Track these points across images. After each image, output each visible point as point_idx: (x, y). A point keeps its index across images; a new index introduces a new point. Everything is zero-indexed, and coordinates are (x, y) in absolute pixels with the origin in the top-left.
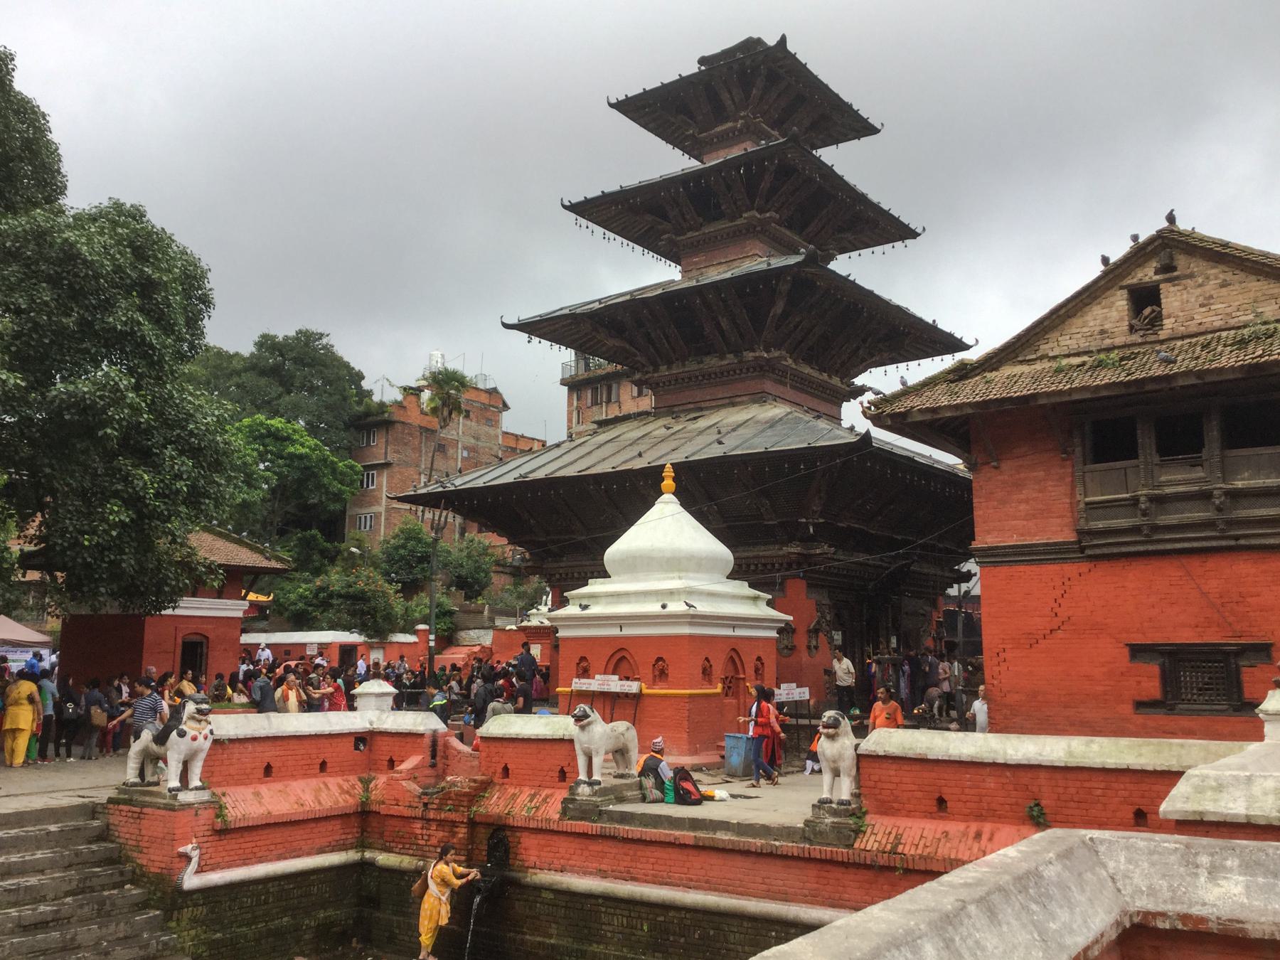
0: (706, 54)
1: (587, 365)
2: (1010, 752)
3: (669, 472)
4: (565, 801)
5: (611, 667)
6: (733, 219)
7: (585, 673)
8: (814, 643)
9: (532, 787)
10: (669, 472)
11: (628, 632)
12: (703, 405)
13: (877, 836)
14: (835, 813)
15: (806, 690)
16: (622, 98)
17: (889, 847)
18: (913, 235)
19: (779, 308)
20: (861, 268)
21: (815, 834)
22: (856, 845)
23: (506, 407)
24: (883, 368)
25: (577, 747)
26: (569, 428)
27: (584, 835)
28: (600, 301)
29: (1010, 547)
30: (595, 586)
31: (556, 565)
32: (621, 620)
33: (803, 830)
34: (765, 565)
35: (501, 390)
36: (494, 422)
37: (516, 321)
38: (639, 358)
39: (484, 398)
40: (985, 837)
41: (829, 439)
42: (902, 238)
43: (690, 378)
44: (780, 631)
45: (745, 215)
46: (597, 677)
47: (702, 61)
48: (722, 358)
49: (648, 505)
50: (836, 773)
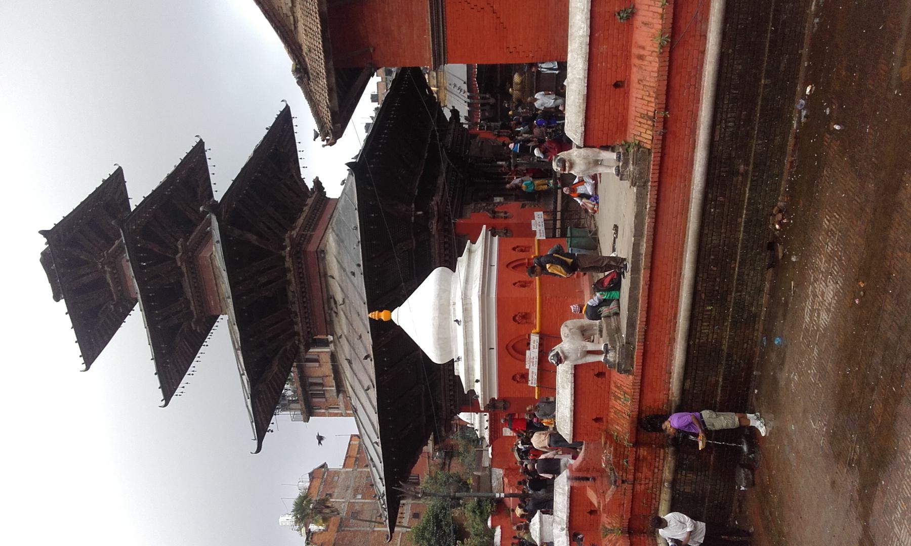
0: (52, 295)
1: (293, 402)
2: (581, 33)
3: (375, 315)
4: (620, 371)
5: (520, 356)
6: (182, 275)
7: (525, 376)
8: (502, 215)
9: (609, 399)
10: (375, 315)
11: (494, 344)
12: (325, 298)
13: (642, 132)
14: (626, 163)
15: (536, 214)
16: (82, 360)
17: (650, 122)
18: (201, 144)
19: (253, 238)
20: (222, 178)
21: (642, 178)
22: (649, 147)
23: (324, 466)
24: (301, 169)
25: (580, 362)
26: (341, 415)
27: (645, 355)
28: (241, 375)
29: (433, 41)
30: (460, 370)
31: (444, 409)
33: (638, 186)
34: (445, 249)
35: (311, 470)
36: (336, 473)
37: (256, 442)
38: (288, 347)
39: (317, 482)
40: (642, 52)
41: (353, 197)
42: (203, 151)
43: (305, 307)
44: (493, 235)
45: (179, 264)
46: (527, 367)
47: (57, 298)
48: (289, 282)
50: (597, 163)
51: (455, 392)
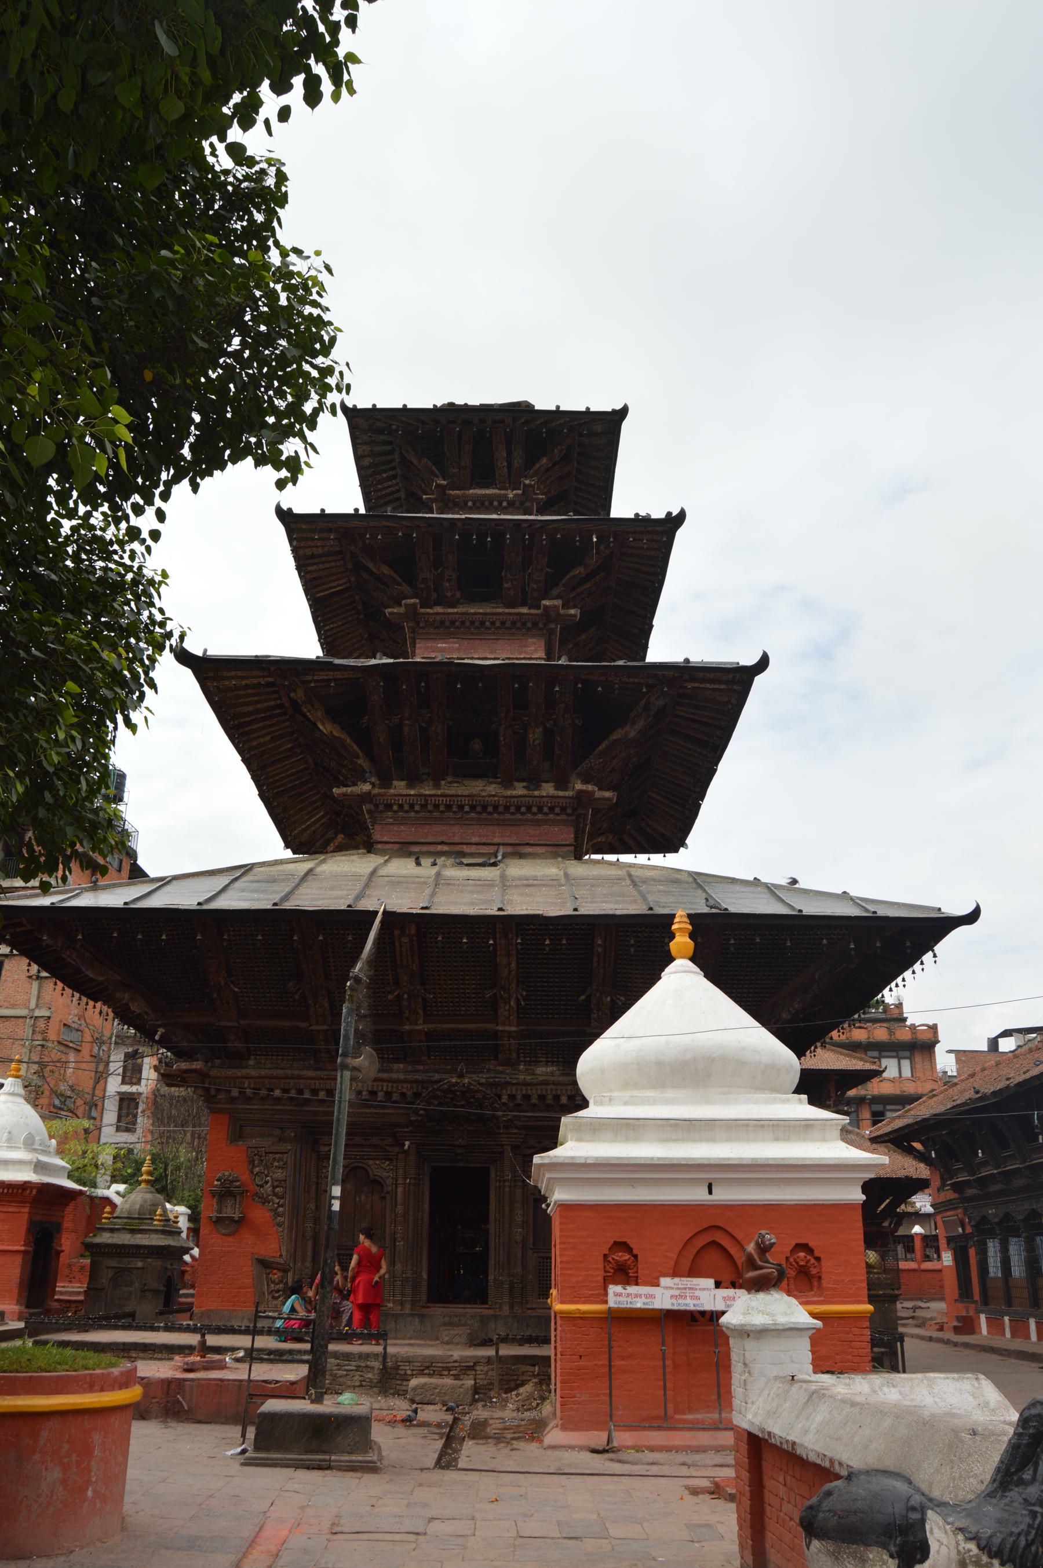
5: (687, 1262)
11: (723, 1195)
12: (466, 849)
31: (239, 1073)
32: (711, 1173)
38: (360, 761)
46: (665, 1281)
48: (507, 784)
49: (653, 978)
51: (277, 1100)
